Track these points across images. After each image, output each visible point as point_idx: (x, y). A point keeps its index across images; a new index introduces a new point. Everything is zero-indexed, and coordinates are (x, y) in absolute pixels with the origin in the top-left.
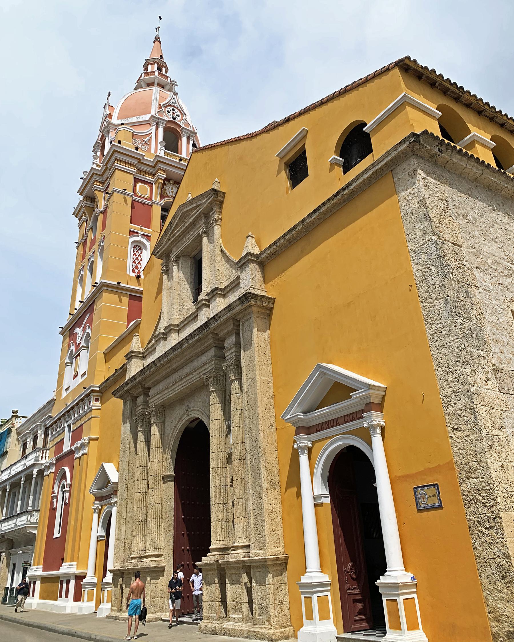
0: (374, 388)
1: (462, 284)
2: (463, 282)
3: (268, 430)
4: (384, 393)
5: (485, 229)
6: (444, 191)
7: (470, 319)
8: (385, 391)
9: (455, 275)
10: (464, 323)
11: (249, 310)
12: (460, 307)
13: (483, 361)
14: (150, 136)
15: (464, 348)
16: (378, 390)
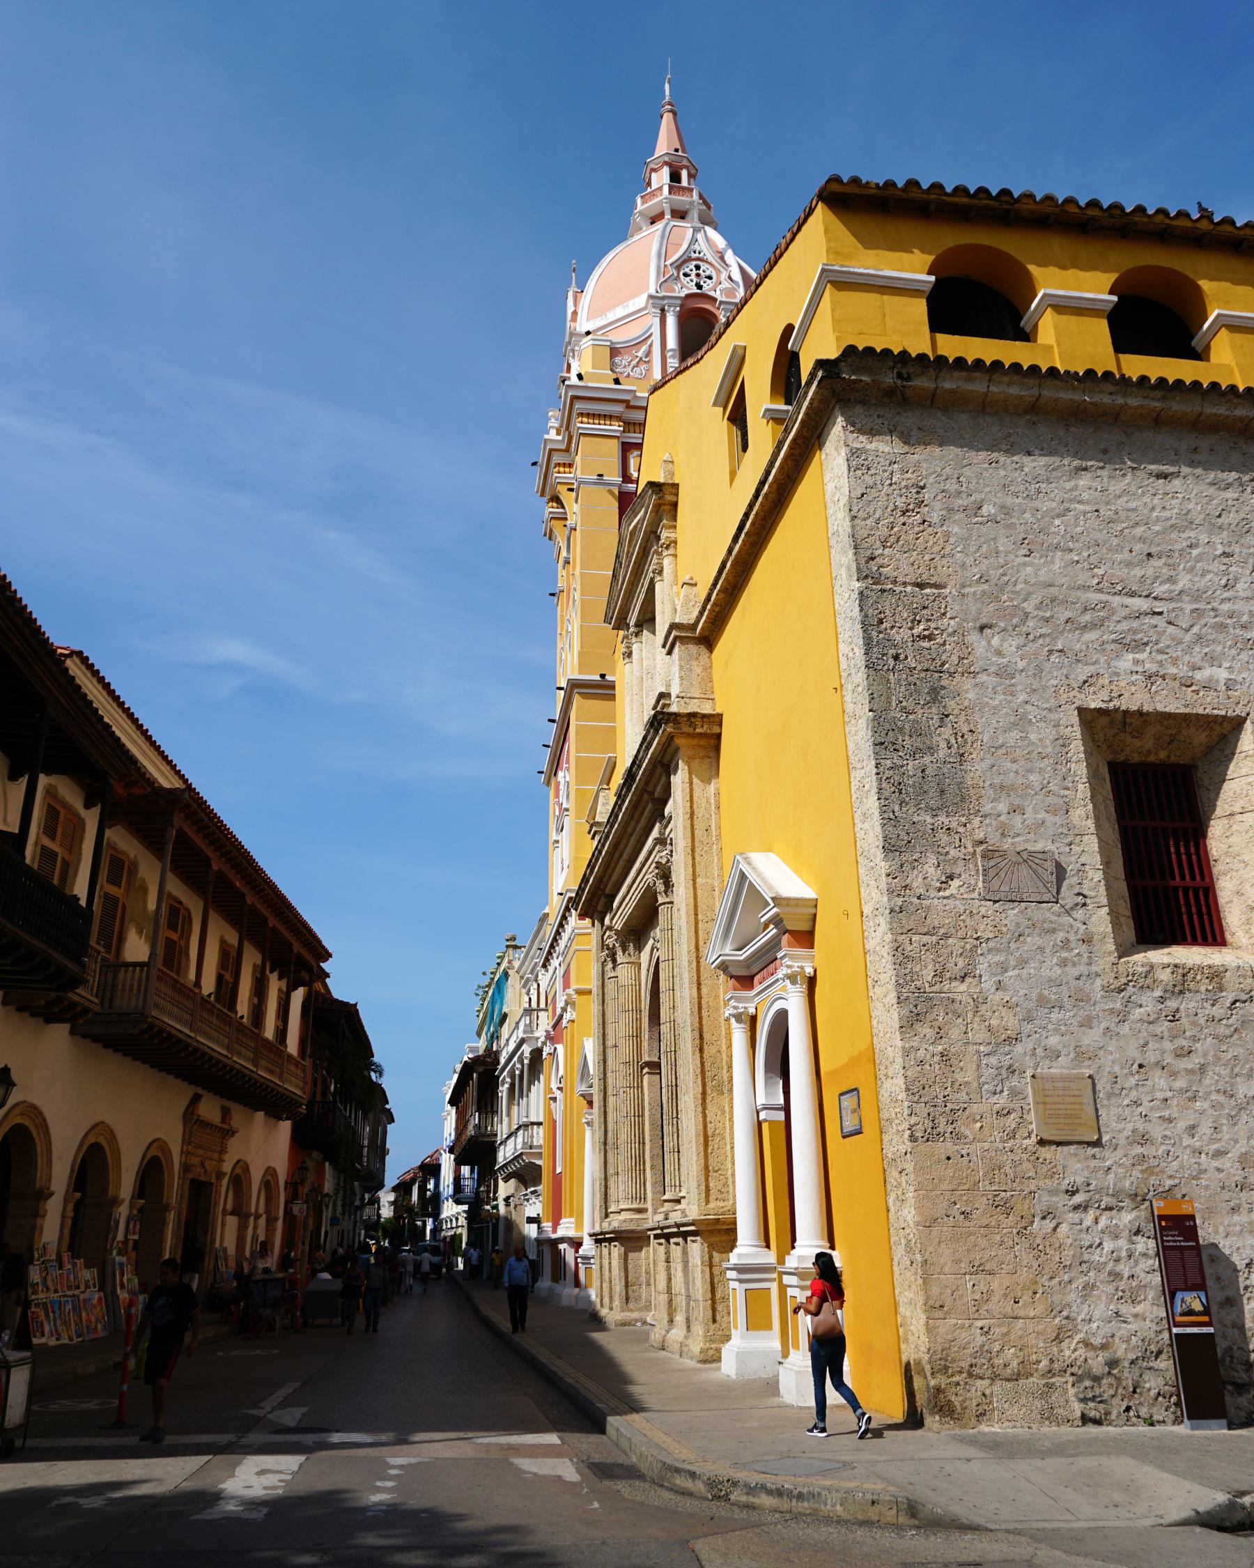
0: (785, 902)
1: (923, 675)
2: (927, 670)
3: (709, 982)
4: (813, 911)
5: (1035, 526)
6: (917, 465)
7: (931, 749)
8: (816, 906)
9: (906, 657)
10: (905, 762)
11: (671, 749)
12: (901, 729)
13: (943, 838)
14: (649, 342)
15: (892, 816)
16: (797, 905)
